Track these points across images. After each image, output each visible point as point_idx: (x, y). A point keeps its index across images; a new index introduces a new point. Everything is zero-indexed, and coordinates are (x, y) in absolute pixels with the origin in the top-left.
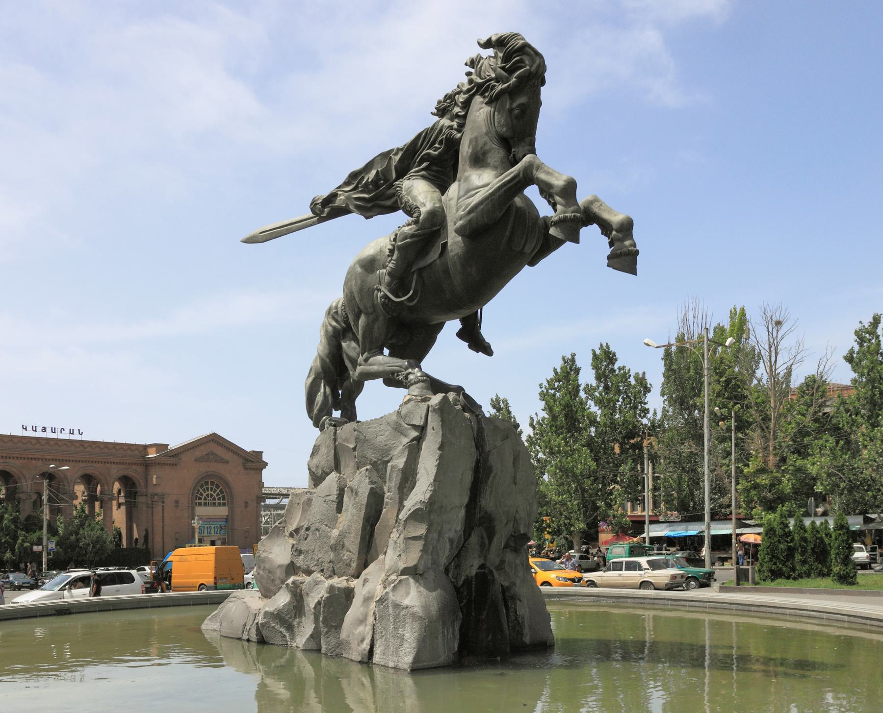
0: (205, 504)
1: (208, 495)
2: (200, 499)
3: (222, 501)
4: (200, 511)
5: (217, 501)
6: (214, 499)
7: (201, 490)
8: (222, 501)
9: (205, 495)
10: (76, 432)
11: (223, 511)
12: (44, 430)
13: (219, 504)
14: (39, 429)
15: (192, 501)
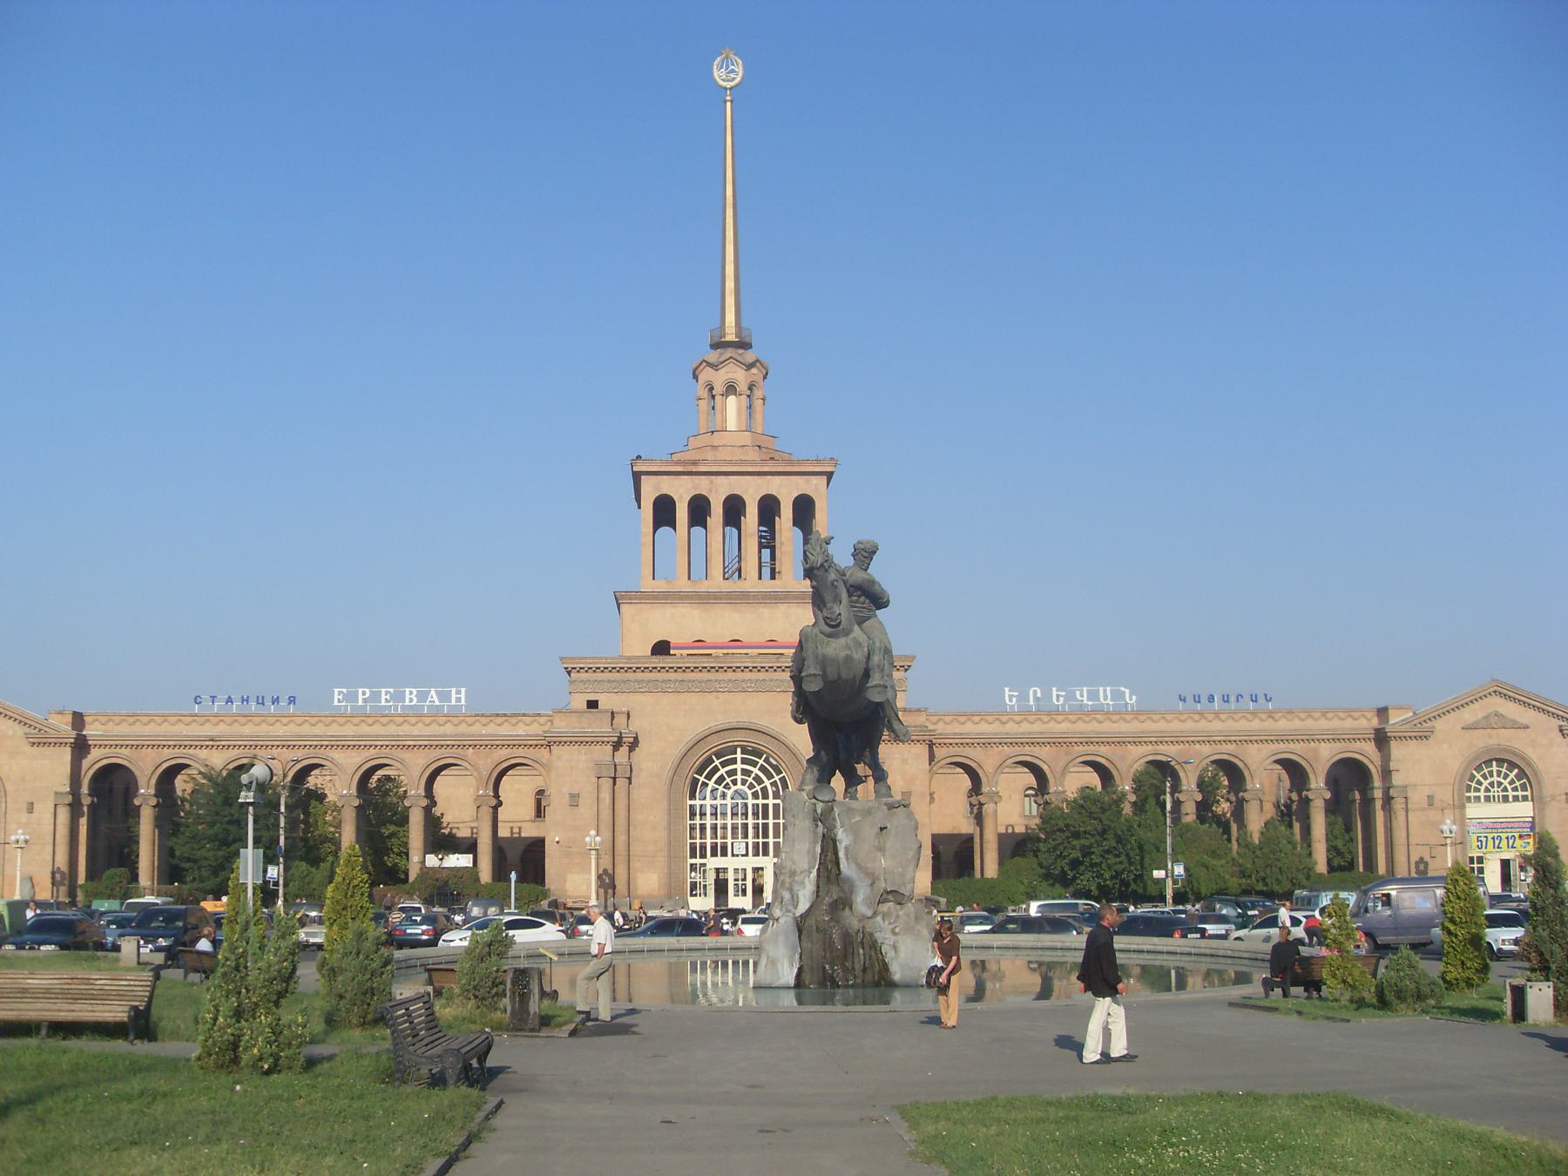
0: (1487, 799)
1: (1492, 784)
2: (1478, 790)
3: (1520, 793)
4: (1473, 811)
5: (1511, 794)
6: (1505, 789)
7: (1478, 776)
8: (1520, 793)
9: (1485, 783)
10: (1261, 700)
11: (1525, 810)
12: (1211, 699)
13: (1516, 799)
14: (1204, 700)
15: (1461, 795)
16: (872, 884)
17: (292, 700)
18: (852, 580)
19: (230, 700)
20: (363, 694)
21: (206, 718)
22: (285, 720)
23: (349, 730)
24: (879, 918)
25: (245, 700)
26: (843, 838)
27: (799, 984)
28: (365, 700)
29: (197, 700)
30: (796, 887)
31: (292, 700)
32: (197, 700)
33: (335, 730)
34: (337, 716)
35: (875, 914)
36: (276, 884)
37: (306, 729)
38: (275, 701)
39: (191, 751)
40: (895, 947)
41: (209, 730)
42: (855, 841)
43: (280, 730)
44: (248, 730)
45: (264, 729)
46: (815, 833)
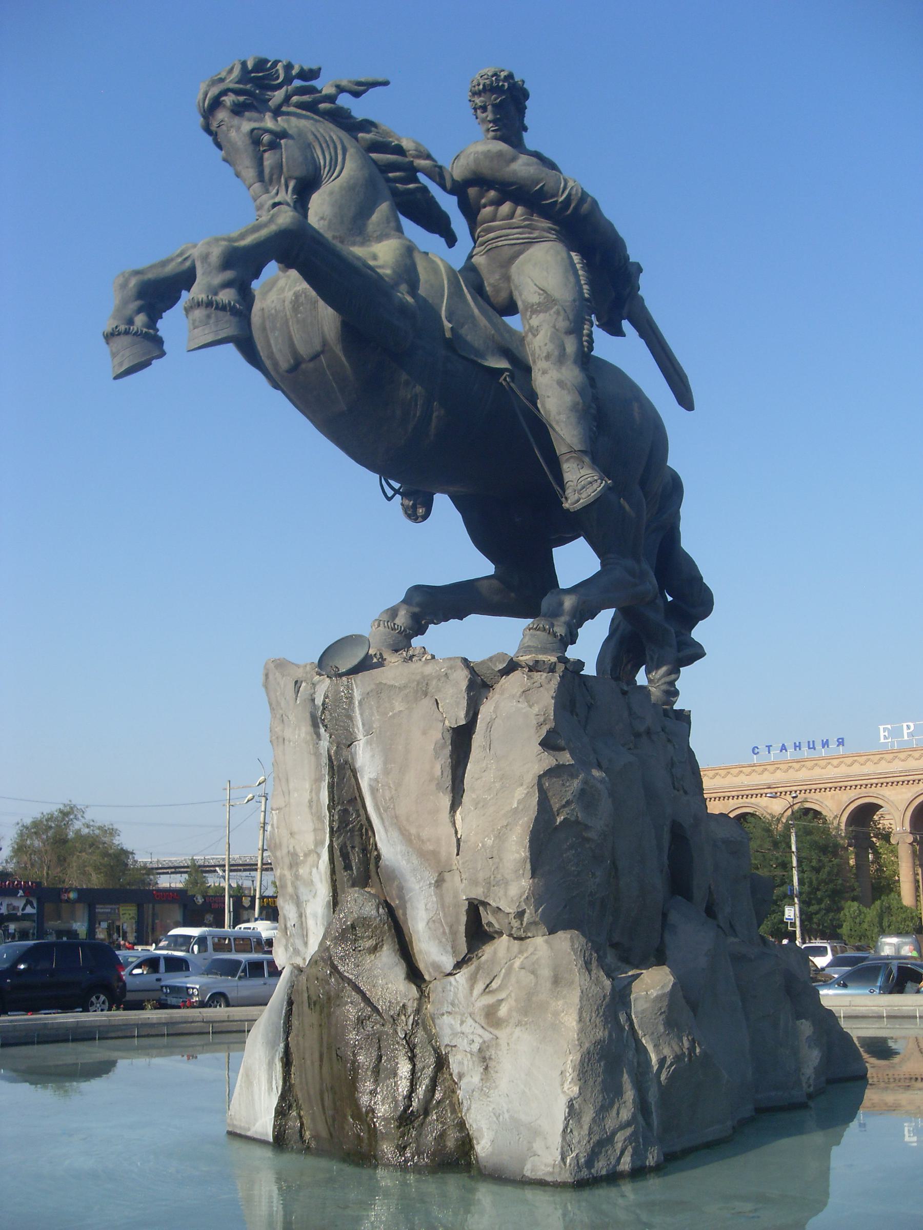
16: (439, 882)
17: (841, 742)
18: (457, 171)
19: (784, 748)
20: (907, 728)
21: (764, 767)
22: (835, 762)
23: (897, 766)
24: (461, 977)
25: (797, 746)
26: (367, 761)
27: (280, 1141)
28: (911, 735)
29: (755, 751)
30: (303, 890)
31: (841, 742)
32: (755, 751)
33: (884, 767)
34: (883, 753)
35: (459, 965)
36: (793, 925)
37: (856, 769)
38: (825, 744)
39: (754, 800)
40: (484, 1058)
41: (767, 778)
42: (386, 772)
43: (832, 772)
44: (803, 774)
45: (817, 773)
46: (317, 755)
